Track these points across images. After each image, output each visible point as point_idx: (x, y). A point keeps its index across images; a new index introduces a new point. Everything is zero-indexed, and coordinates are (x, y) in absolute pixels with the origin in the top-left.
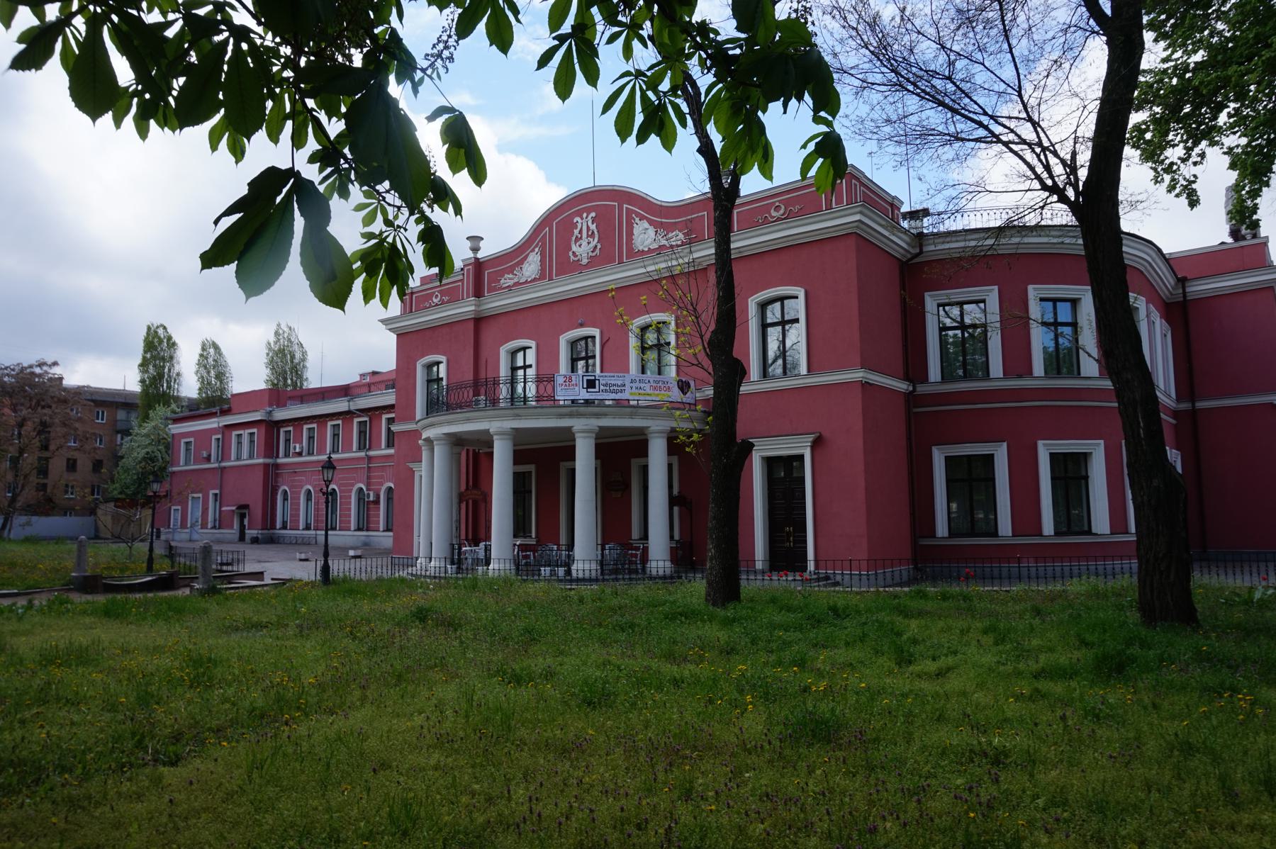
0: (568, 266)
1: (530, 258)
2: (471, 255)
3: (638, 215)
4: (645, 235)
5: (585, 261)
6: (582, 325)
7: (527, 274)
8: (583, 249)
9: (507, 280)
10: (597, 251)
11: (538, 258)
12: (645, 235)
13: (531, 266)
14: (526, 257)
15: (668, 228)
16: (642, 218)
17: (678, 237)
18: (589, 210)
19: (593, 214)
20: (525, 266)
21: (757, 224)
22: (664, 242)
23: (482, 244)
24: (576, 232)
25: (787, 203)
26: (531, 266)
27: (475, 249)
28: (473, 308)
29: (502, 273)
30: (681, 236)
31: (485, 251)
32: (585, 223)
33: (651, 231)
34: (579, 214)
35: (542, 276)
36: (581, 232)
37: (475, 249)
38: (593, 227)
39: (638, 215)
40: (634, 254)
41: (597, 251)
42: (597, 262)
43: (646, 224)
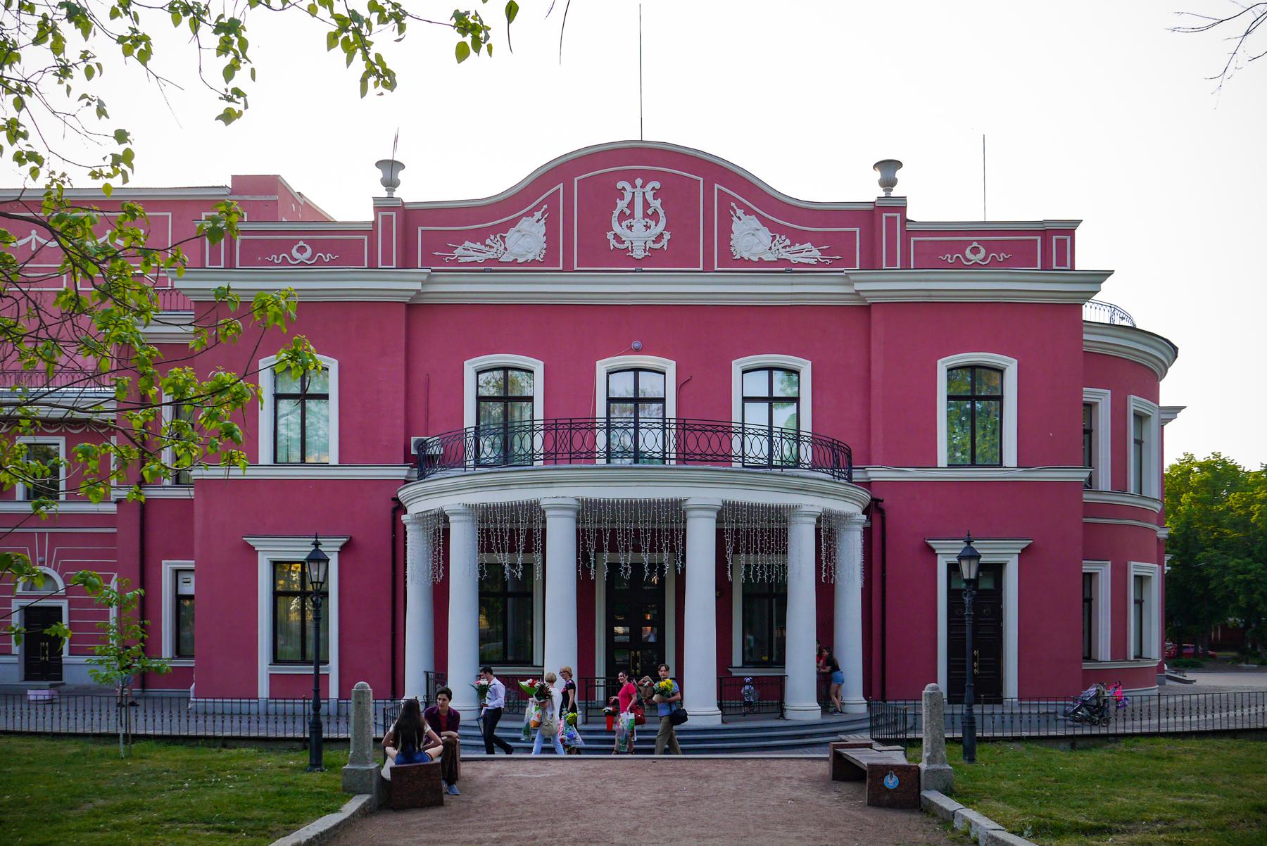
0: (601, 254)
1: (525, 224)
2: (383, 193)
3: (741, 205)
4: (750, 238)
5: (639, 253)
6: (637, 352)
7: (516, 250)
8: (638, 235)
9: (468, 252)
10: (664, 242)
11: (541, 229)
12: (750, 238)
13: (527, 239)
14: (514, 223)
15: (797, 237)
16: (748, 212)
17: (809, 253)
18: (647, 177)
19: (657, 185)
20: (512, 235)
21: (944, 265)
22: (785, 256)
23: (401, 175)
24: (622, 205)
26: (527, 239)
27: (391, 183)
28: (418, 286)
29: (460, 238)
30: (816, 253)
31: (411, 191)
32: (638, 193)
33: (765, 235)
34: (630, 177)
35: (550, 256)
36: (631, 205)
37: (391, 183)
38: (656, 204)
39: (741, 205)
40: (731, 262)
41: (664, 242)
42: (655, 259)
43: (753, 222)
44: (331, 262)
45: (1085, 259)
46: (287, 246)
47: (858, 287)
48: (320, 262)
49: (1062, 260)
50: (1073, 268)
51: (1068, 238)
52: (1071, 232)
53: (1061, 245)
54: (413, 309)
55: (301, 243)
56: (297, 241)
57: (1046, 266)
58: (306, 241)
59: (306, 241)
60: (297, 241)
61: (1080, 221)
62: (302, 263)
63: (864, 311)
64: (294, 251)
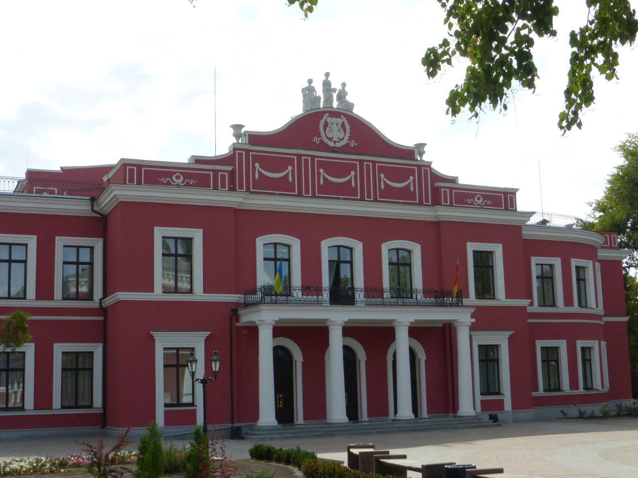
25: (485, 197)
28: (241, 200)
44: (194, 185)
45: (522, 205)
46: (170, 175)
47: (439, 213)
48: (188, 185)
49: (512, 206)
50: (516, 210)
51: (514, 196)
52: (515, 194)
53: (511, 198)
54: (237, 213)
55: (178, 174)
56: (176, 172)
57: (506, 209)
58: (180, 173)
59: (180, 173)
60: (176, 172)
61: (517, 190)
62: (178, 185)
63: (437, 225)
64: (174, 178)
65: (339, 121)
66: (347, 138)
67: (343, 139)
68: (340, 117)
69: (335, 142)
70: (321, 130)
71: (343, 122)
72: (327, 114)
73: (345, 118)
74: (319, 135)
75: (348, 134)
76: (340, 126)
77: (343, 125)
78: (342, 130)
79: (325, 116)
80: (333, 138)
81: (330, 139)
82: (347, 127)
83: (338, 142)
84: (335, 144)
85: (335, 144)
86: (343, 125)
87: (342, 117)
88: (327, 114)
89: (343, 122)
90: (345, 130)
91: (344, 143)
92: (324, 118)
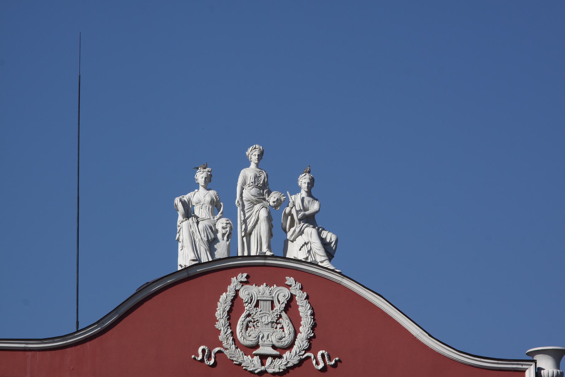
65: (281, 294)
66: (301, 341)
67: (290, 347)
68: (282, 283)
69: (263, 358)
70: (221, 324)
71: (292, 297)
72: (242, 277)
73: (299, 285)
74: (213, 338)
75: (305, 331)
76: (279, 307)
77: (290, 305)
78: (285, 321)
79: (235, 282)
80: (257, 346)
81: (250, 349)
82: (304, 310)
83: (274, 357)
84: (263, 364)
85: (263, 364)
86: (290, 305)
87: (290, 280)
88: (242, 277)
89: (292, 297)
90: (296, 322)
91: (290, 358)
92: (231, 289)
